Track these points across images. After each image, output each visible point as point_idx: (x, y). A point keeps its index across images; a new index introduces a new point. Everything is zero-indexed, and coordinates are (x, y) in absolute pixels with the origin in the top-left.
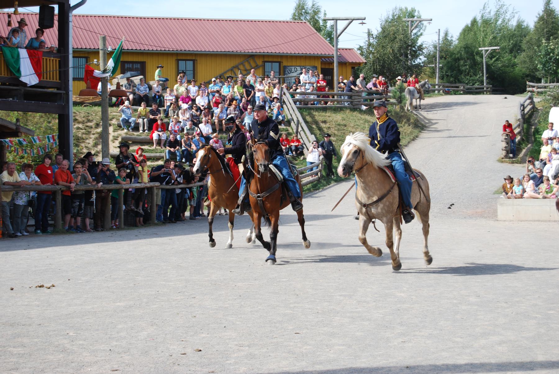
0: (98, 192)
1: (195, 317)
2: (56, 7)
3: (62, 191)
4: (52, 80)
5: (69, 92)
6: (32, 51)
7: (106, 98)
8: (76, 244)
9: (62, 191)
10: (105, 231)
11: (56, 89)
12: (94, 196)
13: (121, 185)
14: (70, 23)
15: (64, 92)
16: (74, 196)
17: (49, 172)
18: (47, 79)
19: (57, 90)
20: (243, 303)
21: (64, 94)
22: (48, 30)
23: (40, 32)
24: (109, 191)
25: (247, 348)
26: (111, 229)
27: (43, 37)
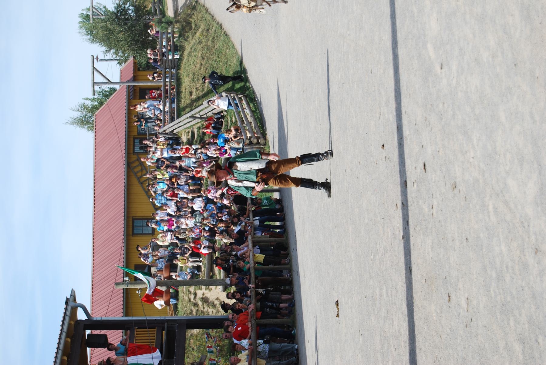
0: (257, 287)
1: (359, 162)
2: (88, 332)
3: (257, 319)
4: (155, 335)
5: (166, 320)
6: (129, 353)
7: (171, 282)
8: (298, 259)
9: (257, 319)
10: (292, 276)
11: (164, 332)
12: (261, 291)
13: (251, 268)
14: (102, 319)
15: (166, 324)
16: (261, 309)
17: (239, 329)
18: (154, 339)
19: (164, 331)
20: (350, 127)
21: (167, 324)
22: (109, 340)
23: (110, 347)
24: (256, 278)
25: (382, 108)
26: (291, 275)
27: (115, 345)
